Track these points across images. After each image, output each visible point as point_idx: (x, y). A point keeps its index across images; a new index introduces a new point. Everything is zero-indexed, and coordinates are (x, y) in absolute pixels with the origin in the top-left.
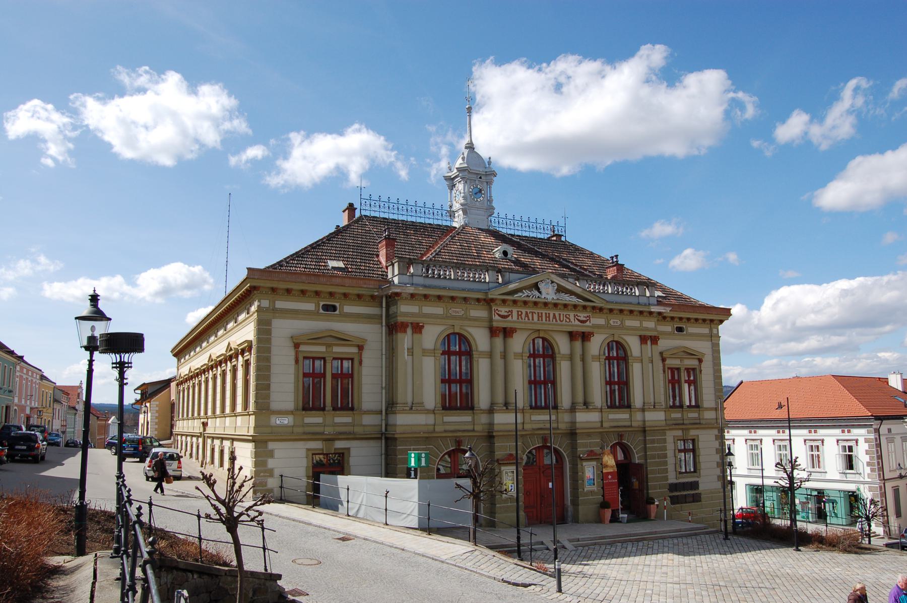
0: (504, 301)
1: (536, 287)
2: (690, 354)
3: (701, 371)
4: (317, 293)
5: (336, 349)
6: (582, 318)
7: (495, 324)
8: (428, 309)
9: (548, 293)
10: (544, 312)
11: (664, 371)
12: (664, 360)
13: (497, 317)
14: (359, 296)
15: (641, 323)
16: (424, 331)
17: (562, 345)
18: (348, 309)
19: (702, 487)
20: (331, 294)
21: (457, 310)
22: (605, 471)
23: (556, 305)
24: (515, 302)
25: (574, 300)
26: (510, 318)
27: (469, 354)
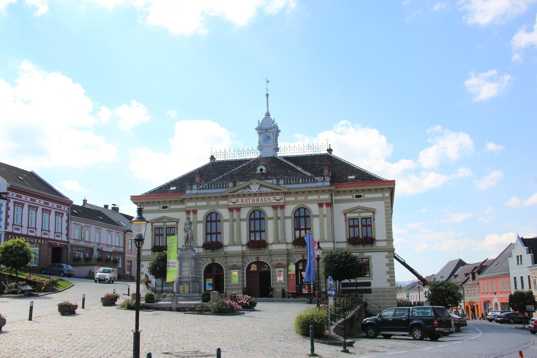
0: (233, 196)
1: (248, 187)
2: (367, 210)
3: (374, 219)
4: (159, 202)
5: (167, 224)
6: (278, 199)
7: (230, 207)
8: (199, 204)
9: (255, 188)
10: (256, 198)
11: (346, 221)
12: (345, 215)
13: (231, 204)
14: (176, 201)
15: (319, 197)
16: (198, 213)
17: (269, 212)
18: (172, 207)
19: (373, 286)
20: (165, 202)
21: (214, 203)
22: (289, 273)
23: (261, 194)
24: (239, 196)
25: (269, 190)
26: (237, 203)
27: (217, 221)
